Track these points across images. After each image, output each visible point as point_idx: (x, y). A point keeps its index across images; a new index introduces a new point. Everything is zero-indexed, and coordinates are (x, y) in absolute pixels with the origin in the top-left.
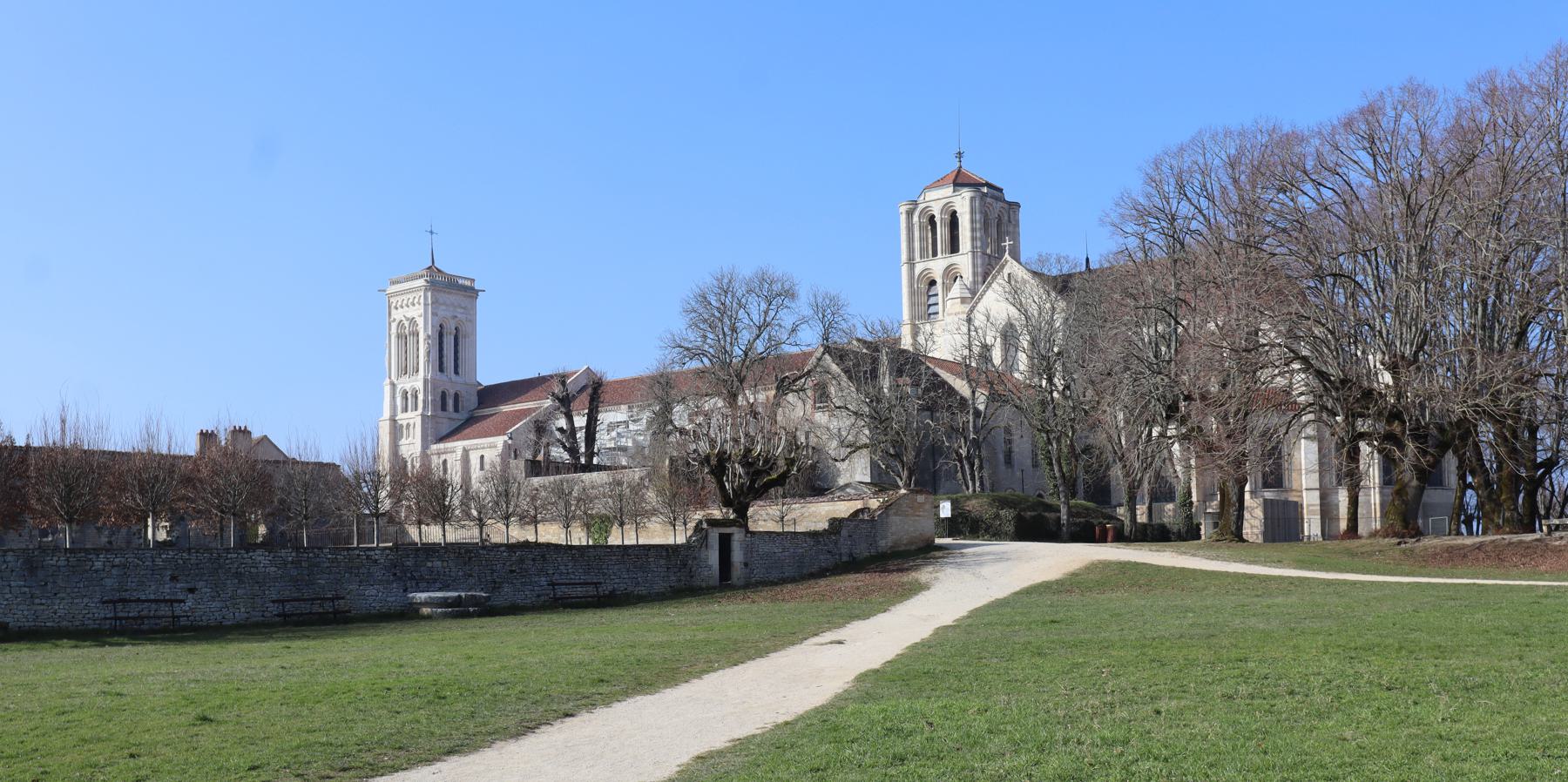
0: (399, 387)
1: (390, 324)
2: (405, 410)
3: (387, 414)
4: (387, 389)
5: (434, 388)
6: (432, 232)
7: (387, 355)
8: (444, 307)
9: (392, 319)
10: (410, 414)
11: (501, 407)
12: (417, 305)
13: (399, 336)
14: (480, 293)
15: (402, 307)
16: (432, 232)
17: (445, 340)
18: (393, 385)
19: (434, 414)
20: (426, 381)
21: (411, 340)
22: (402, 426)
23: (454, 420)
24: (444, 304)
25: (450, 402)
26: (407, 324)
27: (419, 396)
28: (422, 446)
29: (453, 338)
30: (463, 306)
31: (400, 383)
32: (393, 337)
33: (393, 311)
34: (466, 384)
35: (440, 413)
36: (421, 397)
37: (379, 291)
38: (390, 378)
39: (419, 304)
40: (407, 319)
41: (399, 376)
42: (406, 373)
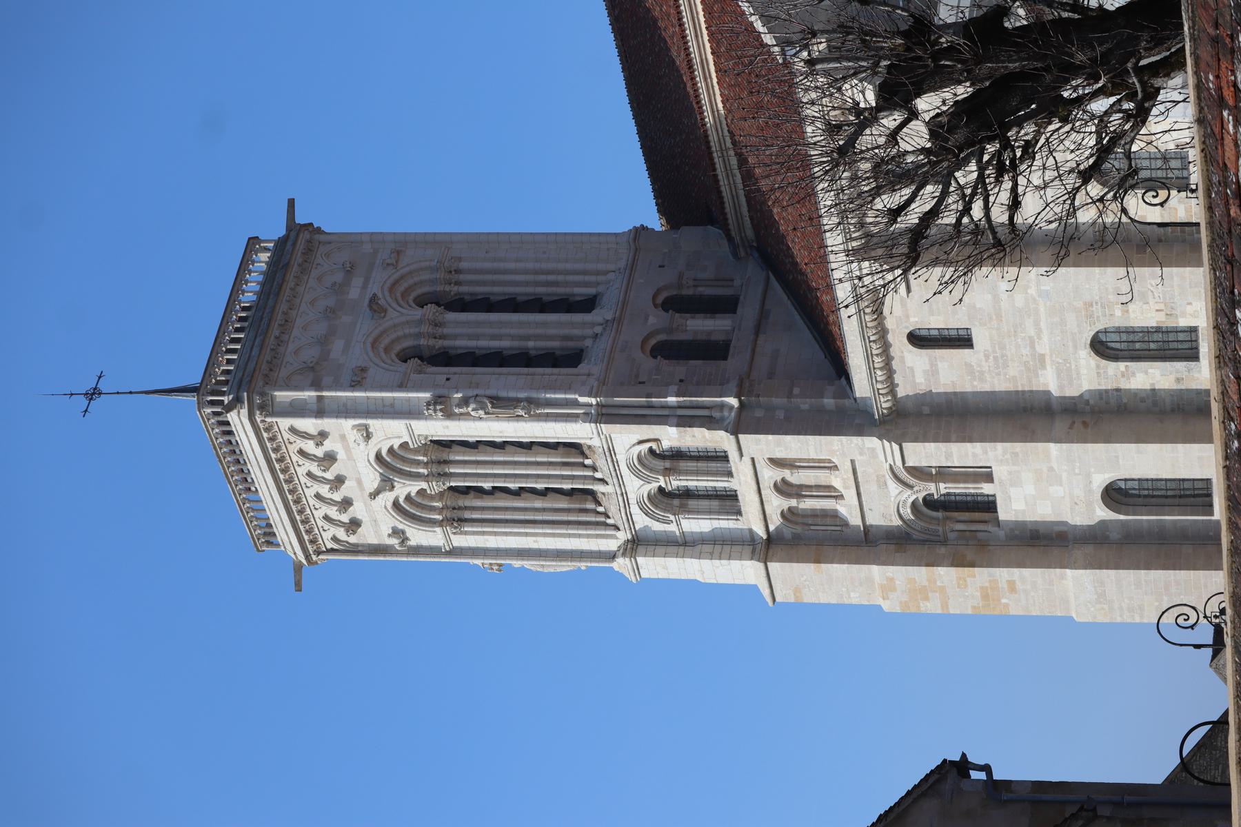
0: (642, 521)
1: (418, 550)
2: (728, 501)
3: (746, 571)
4: (654, 567)
5: (636, 383)
6: (93, 394)
7: (528, 564)
8: (337, 346)
9: (394, 542)
10: (742, 482)
11: (709, 119)
12: (328, 445)
13: (456, 520)
14: (300, 219)
15: (346, 503)
16: (93, 394)
17: (463, 344)
18: (638, 544)
19: (733, 385)
20: (606, 415)
21: (464, 472)
22: (789, 516)
23: (763, 315)
24: (324, 342)
25: (699, 326)
26: (405, 489)
27: (666, 444)
28: (860, 432)
29: (452, 316)
30: (339, 277)
31: (630, 518)
32: (459, 541)
33: (367, 535)
34: (632, 267)
35: (734, 364)
36: (670, 437)
37: (298, 586)
38: (612, 556)
39: (323, 435)
40: (387, 484)
41: (603, 524)
42: (591, 494)
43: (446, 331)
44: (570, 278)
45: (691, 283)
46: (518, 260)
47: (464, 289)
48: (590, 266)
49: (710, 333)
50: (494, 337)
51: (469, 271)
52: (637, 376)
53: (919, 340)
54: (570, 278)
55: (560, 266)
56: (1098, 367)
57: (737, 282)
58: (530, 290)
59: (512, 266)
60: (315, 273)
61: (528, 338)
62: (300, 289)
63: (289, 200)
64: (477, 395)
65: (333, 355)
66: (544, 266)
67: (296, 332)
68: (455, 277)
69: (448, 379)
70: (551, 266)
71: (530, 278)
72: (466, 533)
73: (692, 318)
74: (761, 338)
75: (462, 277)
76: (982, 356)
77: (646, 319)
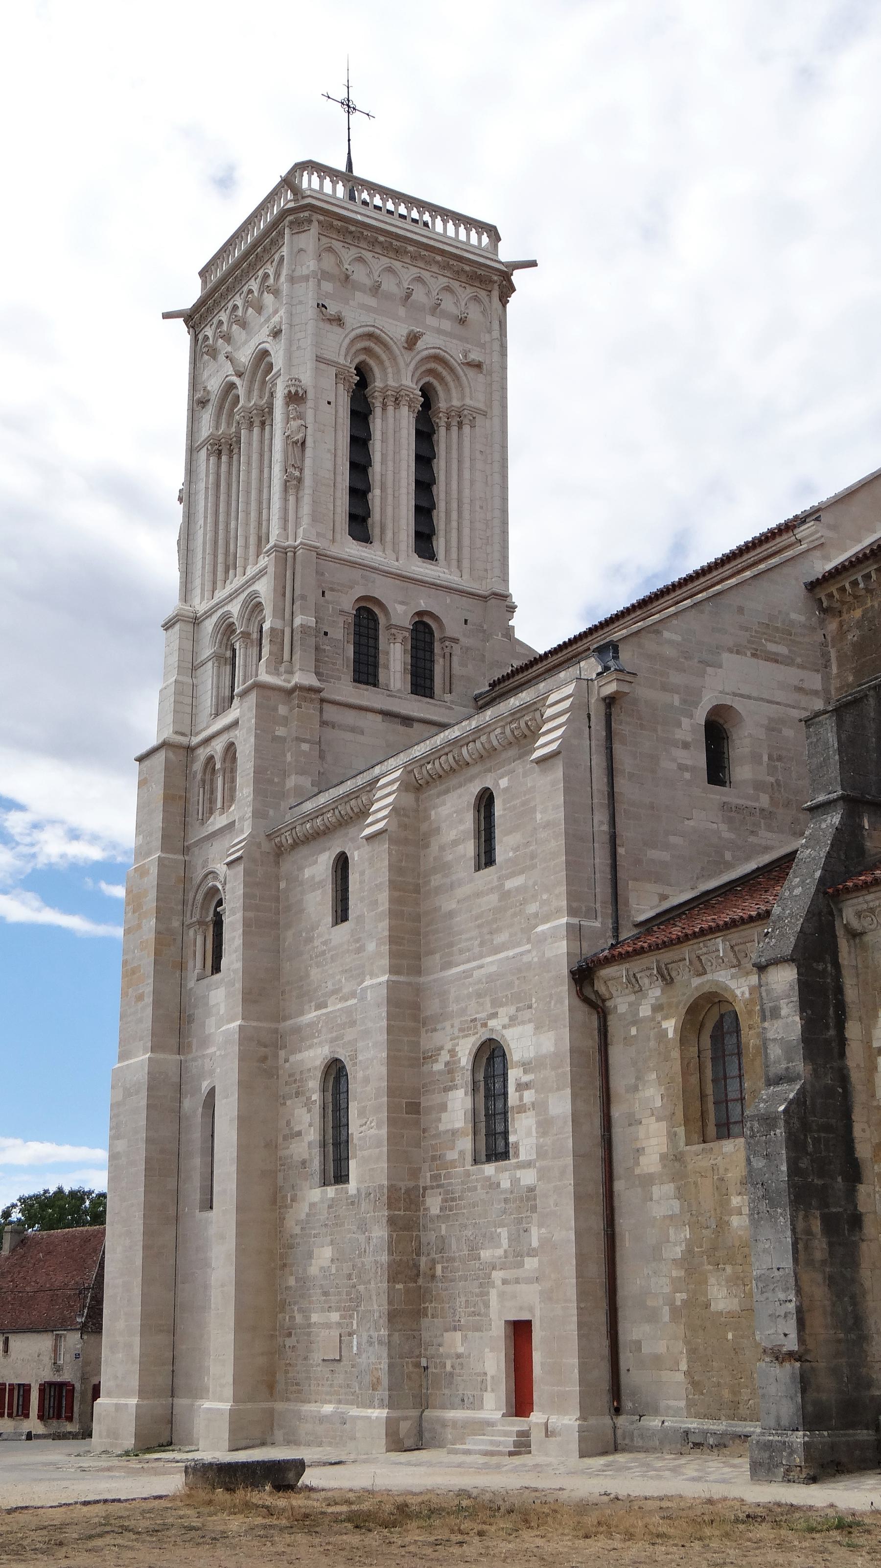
6: (348, 106)
14: (518, 277)
16: (348, 106)
17: (377, 425)
43: (390, 409)
44: (454, 534)
45: (447, 651)
46: (472, 482)
47: (442, 431)
48: (466, 551)
49: (387, 667)
50: (384, 456)
51: (460, 436)
52: (332, 590)
53: (342, 864)
54: (454, 534)
55: (466, 523)
56: (315, 1068)
57: (448, 697)
58: (442, 496)
59: (467, 475)
60: (455, 285)
61: (383, 488)
62: (435, 269)
63: (535, 261)
64: (306, 427)
65: (358, 294)
66: (466, 507)
67: (385, 261)
68: (454, 423)
69: (329, 403)
70: (466, 514)
71: (454, 495)
72: (208, 460)
73: (405, 651)
74: (379, 718)
75: (455, 429)
76: (326, 937)
77: (402, 603)
